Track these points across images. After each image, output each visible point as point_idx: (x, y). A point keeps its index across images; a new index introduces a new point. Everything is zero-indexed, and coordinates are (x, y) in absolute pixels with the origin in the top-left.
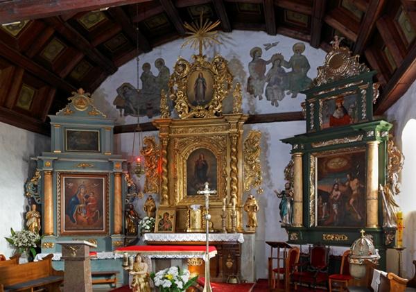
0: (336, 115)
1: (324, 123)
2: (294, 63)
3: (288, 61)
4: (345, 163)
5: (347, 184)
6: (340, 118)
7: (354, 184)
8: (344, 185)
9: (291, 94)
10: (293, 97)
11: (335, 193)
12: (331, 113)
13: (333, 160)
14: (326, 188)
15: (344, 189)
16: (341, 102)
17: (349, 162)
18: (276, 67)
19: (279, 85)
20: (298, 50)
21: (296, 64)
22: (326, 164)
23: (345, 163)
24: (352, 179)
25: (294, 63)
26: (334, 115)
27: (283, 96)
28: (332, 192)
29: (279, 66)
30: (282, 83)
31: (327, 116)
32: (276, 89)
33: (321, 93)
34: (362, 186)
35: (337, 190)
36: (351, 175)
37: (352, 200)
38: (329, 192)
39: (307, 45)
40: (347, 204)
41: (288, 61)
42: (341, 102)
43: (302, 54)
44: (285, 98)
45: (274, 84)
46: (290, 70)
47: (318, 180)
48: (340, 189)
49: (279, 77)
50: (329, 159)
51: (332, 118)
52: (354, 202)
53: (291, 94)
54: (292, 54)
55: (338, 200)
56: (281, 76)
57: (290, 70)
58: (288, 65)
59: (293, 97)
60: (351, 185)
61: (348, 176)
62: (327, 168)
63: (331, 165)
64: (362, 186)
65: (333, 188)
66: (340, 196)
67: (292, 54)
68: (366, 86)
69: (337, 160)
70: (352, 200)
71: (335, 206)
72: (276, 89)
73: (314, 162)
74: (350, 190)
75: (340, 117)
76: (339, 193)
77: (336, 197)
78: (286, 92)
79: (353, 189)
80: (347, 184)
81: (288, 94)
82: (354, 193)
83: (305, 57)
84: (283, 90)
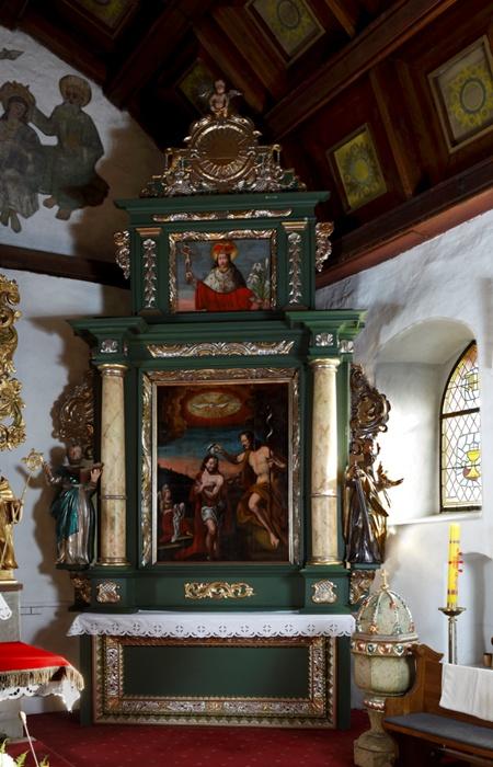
0: (214, 281)
1: (185, 300)
2: (64, 127)
3: (48, 115)
4: (234, 406)
5: (241, 457)
6: (225, 293)
7: (260, 459)
8: (233, 460)
9: (56, 208)
10: (59, 216)
11: (207, 479)
12: (201, 277)
13: (198, 398)
14: (183, 465)
15: (232, 470)
16: (228, 251)
17: (245, 404)
18: (14, 120)
19: (21, 172)
20: (74, 96)
21: (68, 131)
22: (183, 403)
23: (234, 406)
24: (255, 446)
25: (64, 127)
26: (208, 282)
27: (36, 208)
28: (199, 477)
29: (24, 120)
30: (30, 168)
31: (189, 282)
32: (12, 179)
33: (213, 217)
34: (282, 466)
35: (215, 471)
36: (250, 437)
37: (255, 498)
38: (192, 474)
39: (96, 91)
40: (240, 507)
41: (48, 115)
42: (228, 251)
43: (83, 109)
44: (37, 213)
45: (10, 167)
46: (52, 141)
47: (160, 443)
48: (220, 470)
49: (23, 152)
50: (192, 392)
51: (203, 292)
52: (261, 504)
53: (56, 208)
54: (59, 100)
55: (215, 500)
56: (28, 151)
57: (52, 141)
58: (49, 125)
59: (59, 216)
60: (252, 462)
61: (244, 437)
62: (184, 413)
63: (197, 408)
64: (282, 466)
65: (203, 467)
66: (222, 488)
67: (59, 100)
68: (302, 225)
69: (214, 397)
70: (255, 498)
71: (207, 513)
72: (15, 181)
73: (149, 395)
74: (250, 475)
75: (225, 288)
76: (219, 480)
77: (211, 488)
78: (41, 198)
79: (256, 471)
80: (241, 457)
81: (47, 204)
82: (261, 480)
83: (89, 120)
84: (34, 190)
